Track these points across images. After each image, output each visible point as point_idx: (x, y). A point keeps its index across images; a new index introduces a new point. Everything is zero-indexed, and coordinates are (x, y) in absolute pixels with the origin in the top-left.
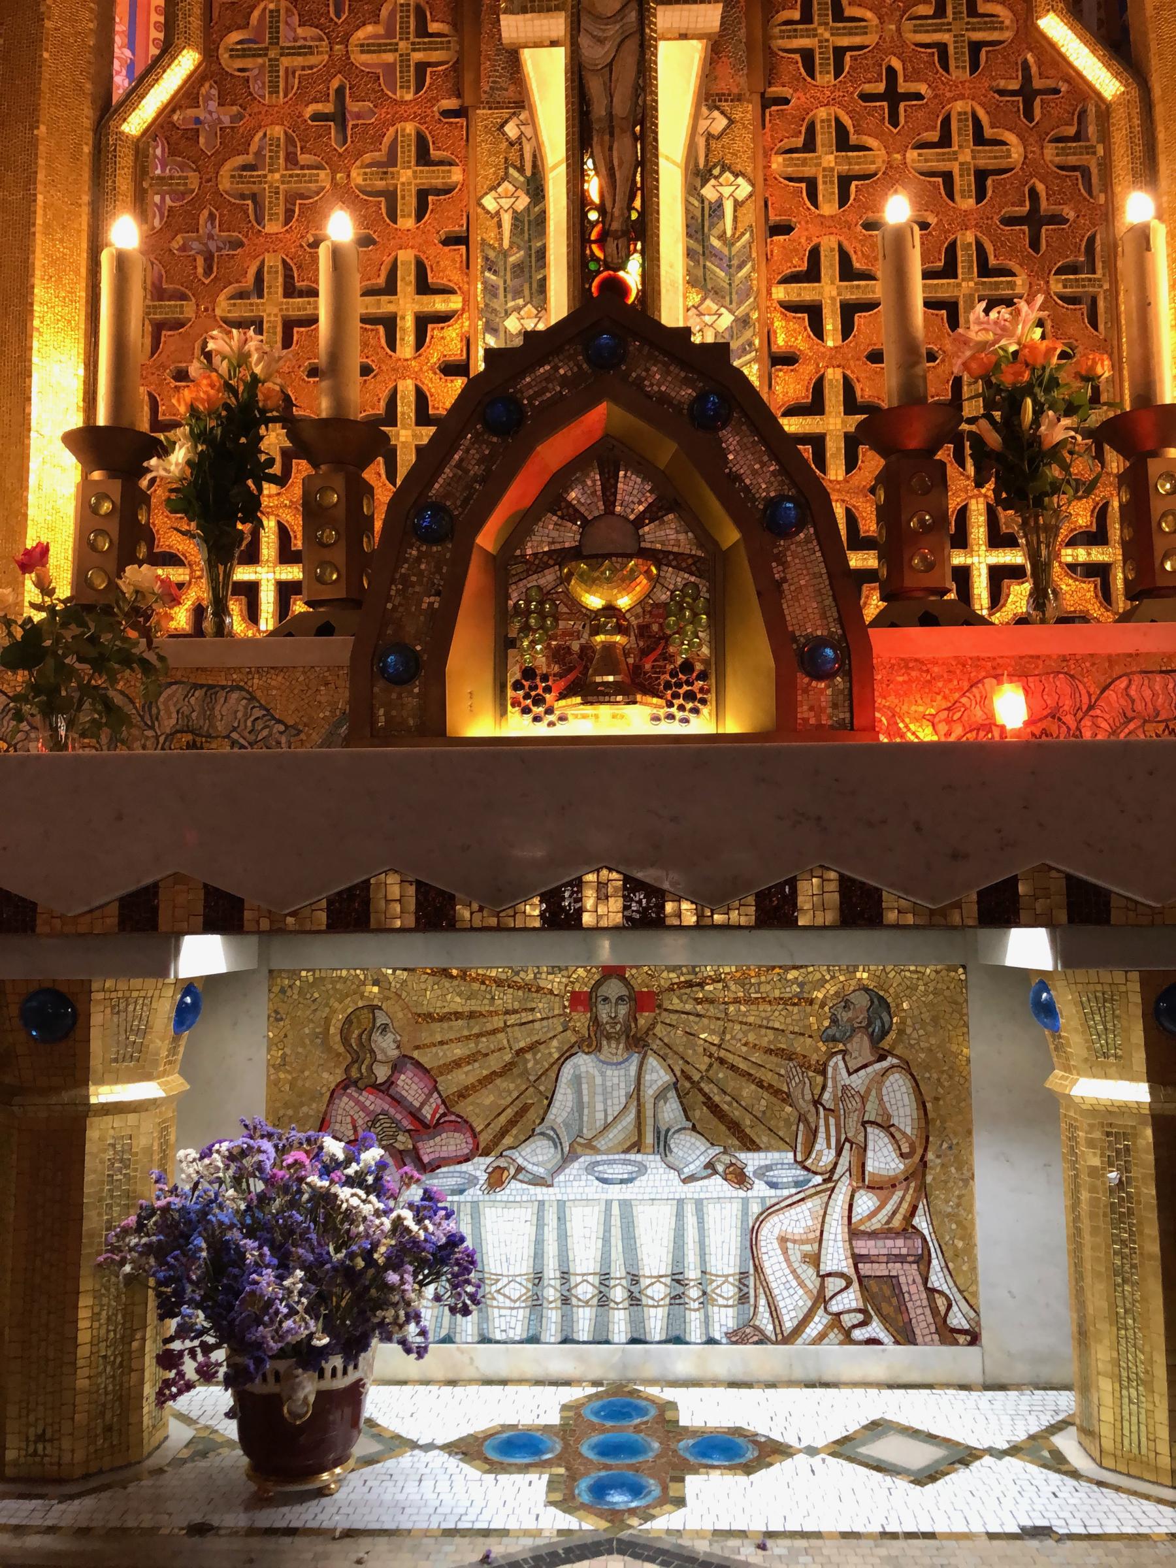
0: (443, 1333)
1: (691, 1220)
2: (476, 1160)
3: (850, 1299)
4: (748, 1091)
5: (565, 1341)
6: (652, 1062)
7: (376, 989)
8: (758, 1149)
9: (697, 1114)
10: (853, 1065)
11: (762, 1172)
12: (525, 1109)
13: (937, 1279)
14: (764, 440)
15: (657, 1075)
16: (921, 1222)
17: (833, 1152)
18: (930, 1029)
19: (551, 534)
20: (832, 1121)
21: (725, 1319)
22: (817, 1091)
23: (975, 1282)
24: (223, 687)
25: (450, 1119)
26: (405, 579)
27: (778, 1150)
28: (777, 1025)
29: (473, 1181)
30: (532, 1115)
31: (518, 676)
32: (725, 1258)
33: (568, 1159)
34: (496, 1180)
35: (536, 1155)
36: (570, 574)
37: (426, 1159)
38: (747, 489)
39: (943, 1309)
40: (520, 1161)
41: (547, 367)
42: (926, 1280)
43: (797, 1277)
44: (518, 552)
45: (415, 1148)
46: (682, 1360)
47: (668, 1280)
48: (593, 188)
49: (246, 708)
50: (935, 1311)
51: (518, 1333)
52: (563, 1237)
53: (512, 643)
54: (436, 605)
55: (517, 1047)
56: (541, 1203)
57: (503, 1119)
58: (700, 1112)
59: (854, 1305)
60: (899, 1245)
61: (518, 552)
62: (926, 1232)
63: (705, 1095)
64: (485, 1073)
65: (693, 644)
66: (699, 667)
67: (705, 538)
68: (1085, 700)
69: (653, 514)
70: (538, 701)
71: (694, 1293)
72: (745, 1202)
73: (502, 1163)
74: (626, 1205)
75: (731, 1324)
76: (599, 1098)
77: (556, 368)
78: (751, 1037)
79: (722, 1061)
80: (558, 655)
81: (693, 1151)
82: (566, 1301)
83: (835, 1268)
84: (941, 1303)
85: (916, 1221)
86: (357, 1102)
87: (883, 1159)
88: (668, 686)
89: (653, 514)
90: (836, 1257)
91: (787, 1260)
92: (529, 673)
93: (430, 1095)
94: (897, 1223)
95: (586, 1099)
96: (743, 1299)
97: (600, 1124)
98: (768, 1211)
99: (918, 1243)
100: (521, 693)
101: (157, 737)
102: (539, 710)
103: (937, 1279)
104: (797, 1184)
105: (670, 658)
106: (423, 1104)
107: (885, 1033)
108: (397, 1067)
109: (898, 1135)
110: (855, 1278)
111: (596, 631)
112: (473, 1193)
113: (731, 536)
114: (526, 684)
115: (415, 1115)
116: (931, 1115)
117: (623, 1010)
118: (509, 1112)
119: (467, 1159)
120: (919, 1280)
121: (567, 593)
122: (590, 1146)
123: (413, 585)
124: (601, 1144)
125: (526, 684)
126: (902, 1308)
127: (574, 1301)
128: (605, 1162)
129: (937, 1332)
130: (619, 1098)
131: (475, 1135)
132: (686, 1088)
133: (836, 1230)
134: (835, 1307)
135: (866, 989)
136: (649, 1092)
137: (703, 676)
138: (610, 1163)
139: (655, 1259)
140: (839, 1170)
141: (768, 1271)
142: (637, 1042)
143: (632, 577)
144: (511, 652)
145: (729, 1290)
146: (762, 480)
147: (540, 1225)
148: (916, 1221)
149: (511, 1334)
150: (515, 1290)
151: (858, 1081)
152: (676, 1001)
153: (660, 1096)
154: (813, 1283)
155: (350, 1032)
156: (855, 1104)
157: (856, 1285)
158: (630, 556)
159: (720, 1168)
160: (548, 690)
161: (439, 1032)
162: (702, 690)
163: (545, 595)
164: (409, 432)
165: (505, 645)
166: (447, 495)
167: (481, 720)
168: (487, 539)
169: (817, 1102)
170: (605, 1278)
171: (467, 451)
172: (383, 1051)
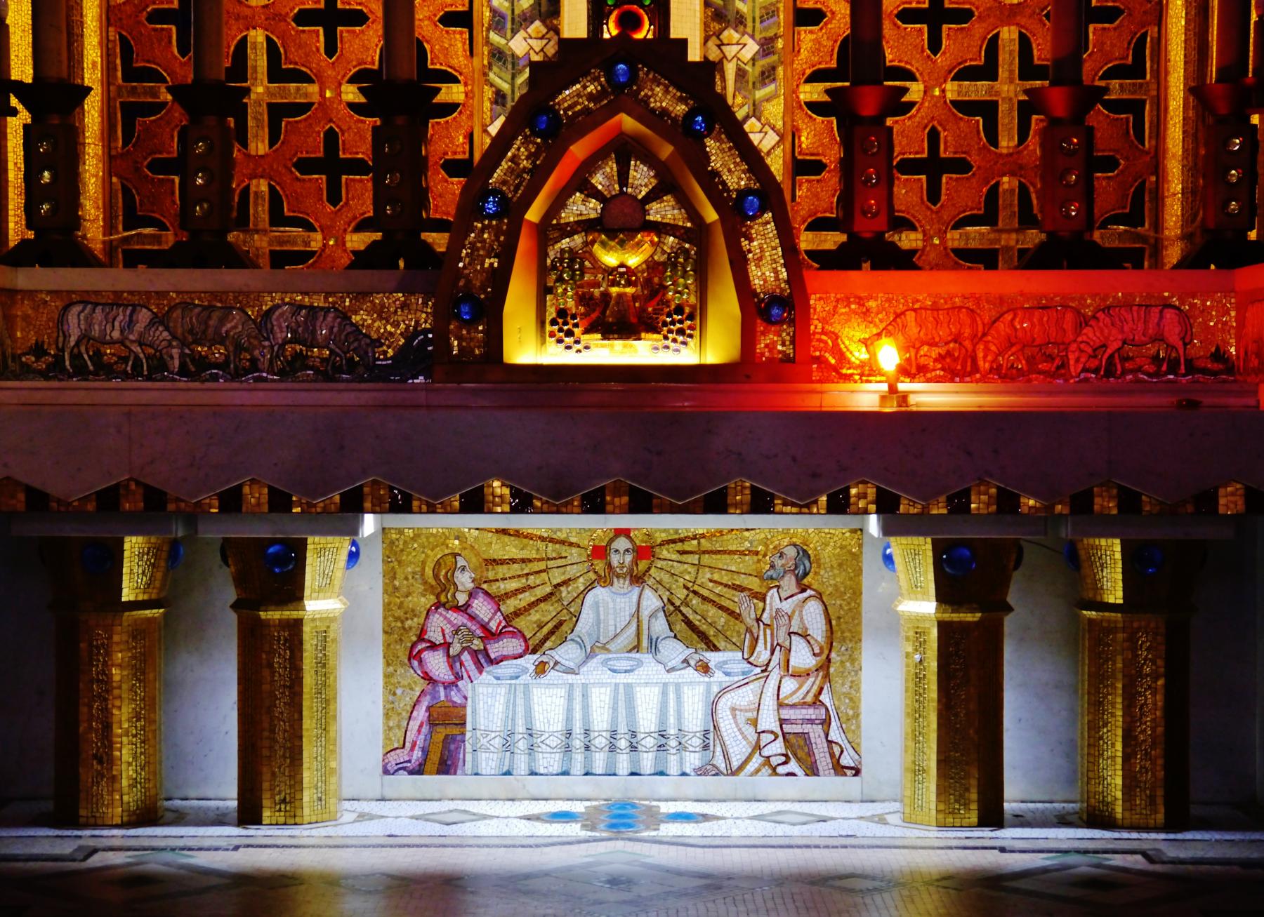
0: (505, 769)
1: (672, 696)
2: (527, 656)
3: (778, 747)
4: (712, 612)
5: (586, 774)
6: (648, 592)
7: (457, 542)
8: (716, 649)
9: (678, 627)
10: (784, 595)
11: (720, 666)
12: (561, 623)
13: (835, 734)
14: (736, 147)
15: (651, 601)
16: (825, 698)
17: (768, 653)
18: (836, 572)
19: (580, 208)
20: (768, 632)
21: (693, 760)
22: (759, 613)
23: (859, 737)
24: (322, 308)
25: (509, 629)
26: (473, 244)
27: (732, 650)
28: (733, 569)
29: (525, 670)
30: (565, 628)
31: (554, 315)
32: (695, 719)
33: (590, 656)
34: (541, 669)
35: (567, 653)
36: (593, 242)
37: (493, 656)
38: (724, 183)
39: (837, 754)
40: (557, 658)
41: (578, 86)
42: (827, 735)
43: (742, 733)
44: (555, 222)
45: (485, 649)
46: (663, 786)
47: (656, 735)
49: (340, 324)
50: (832, 755)
51: (556, 768)
52: (586, 707)
53: (550, 290)
54: (496, 265)
55: (555, 582)
56: (571, 685)
57: (545, 630)
58: (680, 626)
59: (779, 751)
60: (811, 713)
61: (555, 222)
62: (828, 705)
63: (683, 615)
64: (533, 599)
65: (681, 291)
66: (687, 310)
67: (693, 213)
68: (980, 328)
69: (654, 195)
70: (569, 333)
71: (673, 743)
72: (709, 684)
73: (544, 659)
74: (629, 687)
75: (698, 763)
76: (611, 617)
77: (585, 87)
78: (716, 577)
79: (695, 592)
80: (582, 299)
81: (674, 651)
82: (587, 748)
83: (767, 728)
84: (836, 750)
85: (821, 698)
86: (445, 618)
87: (802, 657)
88: (665, 324)
89: (654, 195)
90: (769, 721)
91: (736, 722)
92: (562, 313)
93: (495, 613)
94: (809, 699)
95: (602, 617)
96: (706, 747)
97: (611, 634)
98: (724, 691)
99: (823, 711)
101: (272, 347)
102: (569, 340)
103: (835, 734)
104: (743, 673)
105: (667, 303)
106: (491, 619)
107: (806, 574)
108: (471, 595)
109: (812, 642)
110: (780, 734)
111: (614, 283)
112: (525, 679)
113: (711, 215)
114: (560, 321)
115: (484, 627)
116: (835, 628)
117: (629, 558)
118: (550, 626)
119: (521, 656)
120: (823, 735)
122: (605, 648)
123: (478, 249)
124: (612, 646)
126: (811, 754)
127: (593, 748)
128: (615, 659)
129: (834, 768)
130: (625, 616)
131: (526, 641)
132: (672, 610)
133: (769, 703)
134: (766, 752)
135: (795, 545)
136: (645, 614)
137: (691, 317)
138: (618, 659)
139: (647, 721)
140: (772, 665)
141: (723, 729)
142: (637, 579)
143: (639, 245)
144: (549, 297)
145: (697, 742)
146: (736, 178)
147: (570, 699)
148: (821, 698)
149: (551, 770)
150: (553, 742)
151: (787, 606)
152: (665, 552)
153: (653, 615)
154: (753, 737)
155: (439, 570)
156: (784, 620)
157: (781, 738)
158: (638, 231)
159: (692, 663)
160: (576, 325)
161: (502, 571)
162: (690, 328)
165: (544, 290)
166: (504, 182)
167: (526, 347)
168: (533, 214)
169: (758, 620)
170: (613, 734)
171: (519, 149)
172: (463, 584)
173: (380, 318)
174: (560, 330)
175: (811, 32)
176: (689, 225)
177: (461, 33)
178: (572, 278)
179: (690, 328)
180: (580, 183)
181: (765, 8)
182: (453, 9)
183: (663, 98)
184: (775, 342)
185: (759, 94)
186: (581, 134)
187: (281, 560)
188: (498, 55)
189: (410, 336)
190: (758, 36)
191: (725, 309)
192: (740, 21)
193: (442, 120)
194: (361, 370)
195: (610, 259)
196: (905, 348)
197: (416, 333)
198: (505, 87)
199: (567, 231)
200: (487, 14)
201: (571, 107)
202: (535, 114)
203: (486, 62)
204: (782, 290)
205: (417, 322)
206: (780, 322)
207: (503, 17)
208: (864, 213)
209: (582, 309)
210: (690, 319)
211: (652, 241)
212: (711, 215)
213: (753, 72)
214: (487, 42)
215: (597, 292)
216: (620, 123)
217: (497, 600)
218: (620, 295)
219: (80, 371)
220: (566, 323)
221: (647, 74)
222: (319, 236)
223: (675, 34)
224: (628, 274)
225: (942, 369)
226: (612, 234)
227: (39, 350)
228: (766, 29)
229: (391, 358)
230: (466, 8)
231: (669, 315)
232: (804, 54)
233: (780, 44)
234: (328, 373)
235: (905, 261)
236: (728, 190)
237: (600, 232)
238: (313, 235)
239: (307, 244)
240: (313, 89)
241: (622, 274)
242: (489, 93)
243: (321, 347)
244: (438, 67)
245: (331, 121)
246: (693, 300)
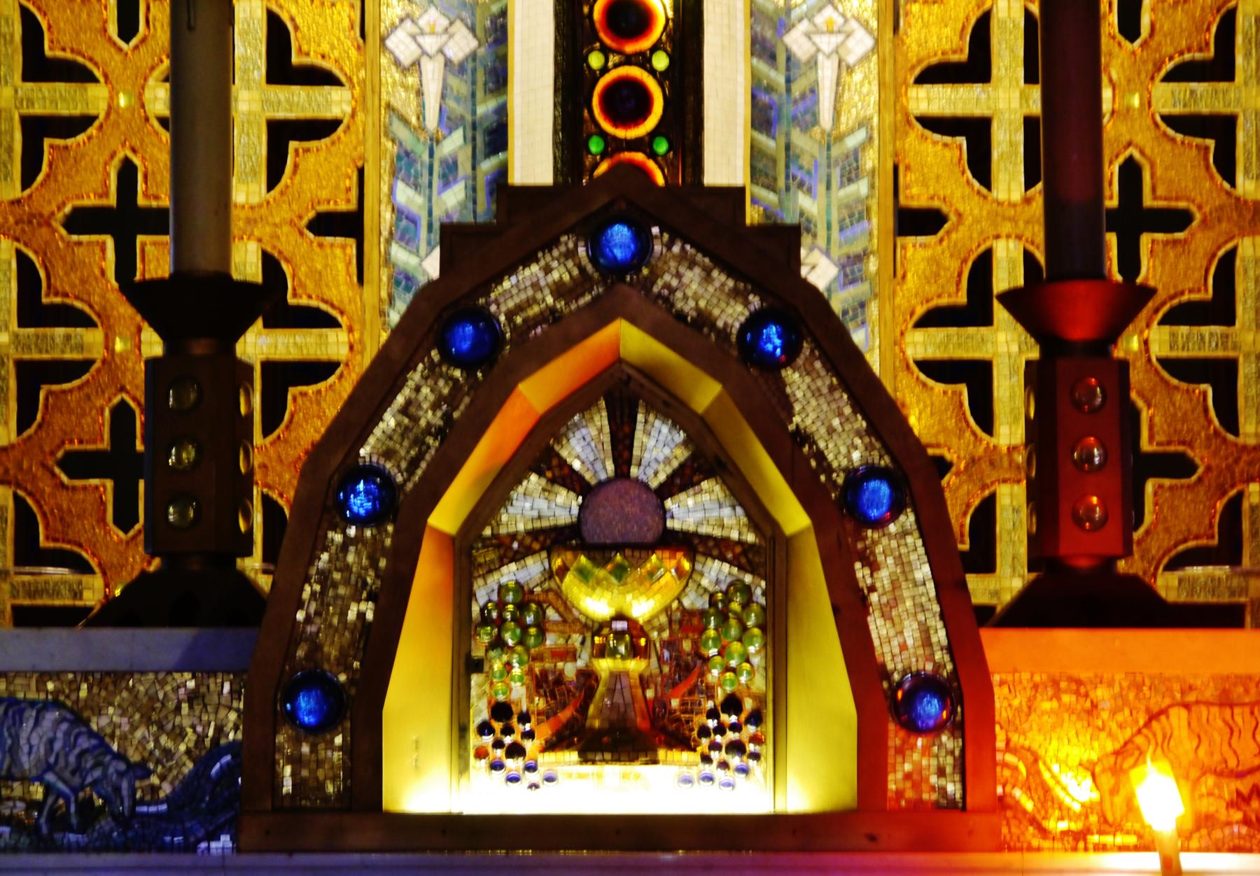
14: (845, 385)
19: (537, 504)
24: (33, 704)
26: (324, 577)
31: (485, 715)
36: (564, 570)
38: (820, 456)
41: (535, 268)
44: (487, 532)
49: (67, 734)
53: (476, 666)
54: (370, 616)
61: (487, 532)
65: (738, 667)
66: (748, 704)
67: (760, 517)
70: (516, 751)
77: (548, 270)
80: (543, 683)
88: (704, 731)
89: (681, 480)
92: (501, 711)
100: (489, 740)
105: (710, 692)
111: (602, 652)
113: (794, 517)
114: (498, 726)
121: (558, 594)
123: (335, 585)
125: (498, 726)
137: (756, 718)
144: (475, 679)
146: (845, 446)
158: (651, 548)
160: (529, 735)
162: (755, 739)
163: (525, 598)
164: (256, 95)
165: (467, 666)
167: (429, 779)
168: (446, 516)
171: (418, 389)
173: (148, 722)
174: (498, 744)
175: (923, 246)
176: (750, 538)
177: (343, 247)
178: (521, 642)
179: (755, 739)
180: (539, 455)
181: (848, 206)
182: (332, 207)
183: (698, 288)
184: (923, 766)
186: (543, 361)
189: (205, 755)
190: (836, 252)
191: (824, 698)
193: (310, 389)
194: (105, 823)
195: (596, 604)
197: (217, 749)
199: (511, 549)
200: (387, 216)
201: (520, 308)
203: (384, 294)
204: (938, 666)
205: (220, 730)
206: (934, 731)
207: (413, 221)
208: (1079, 522)
209: (540, 703)
210: (752, 724)
211: (679, 571)
214: (387, 261)
215: (570, 670)
216: (615, 346)
218: (616, 676)
220: (508, 731)
221: (669, 246)
222: (97, 581)
224: (632, 636)
225: (1246, 821)
226: (600, 552)
228: (849, 242)
229: (167, 800)
230: (353, 206)
231: (713, 714)
232: (912, 281)
233: (872, 265)
236: (829, 470)
237: (576, 550)
238: (86, 579)
239: (77, 594)
240: (93, 338)
241: (619, 635)
243: (26, 780)
244: (304, 301)
245: (123, 389)
246: (760, 684)
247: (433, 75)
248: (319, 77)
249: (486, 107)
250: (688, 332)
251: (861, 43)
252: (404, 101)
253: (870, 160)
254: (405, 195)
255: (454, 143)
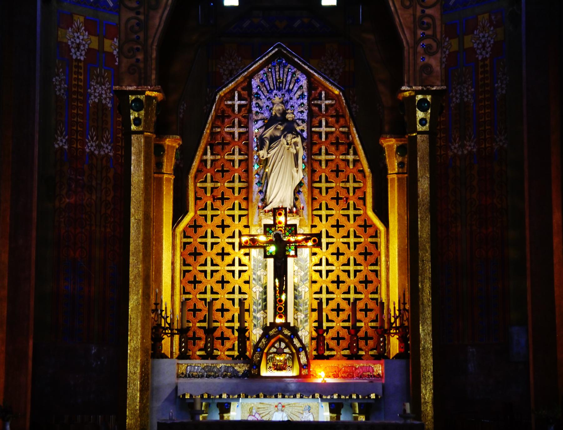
48: (277, 284)
65: (289, 363)
67: (291, 351)
69: (285, 348)
80: (274, 365)
89: (285, 348)
92: (270, 367)
113: (294, 351)
142: (282, 411)
146: (298, 345)
151: (307, 415)
161: (260, 409)
163: (272, 358)
165: (267, 363)
167: (264, 372)
168: (265, 351)
180: (273, 346)
183: (286, 332)
184: (304, 372)
185: (305, 325)
187: (227, 406)
188: (255, 317)
189: (244, 371)
192: (301, 311)
196: (326, 373)
198: (256, 323)
199: (271, 354)
202: (266, 334)
212: (294, 351)
213: (303, 321)
217: (259, 414)
219: (189, 377)
223: (288, 321)
224: (281, 361)
226: (278, 354)
227: (183, 373)
234: (231, 377)
235: (329, 357)
242: (253, 325)
247: (258, 293)
248: (245, 293)
249: (264, 297)
250: (286, 336)
251: (307, 289)
252: (254, 296)
253: (308, 303)
254: (255, 307)
255: (260, 301)
